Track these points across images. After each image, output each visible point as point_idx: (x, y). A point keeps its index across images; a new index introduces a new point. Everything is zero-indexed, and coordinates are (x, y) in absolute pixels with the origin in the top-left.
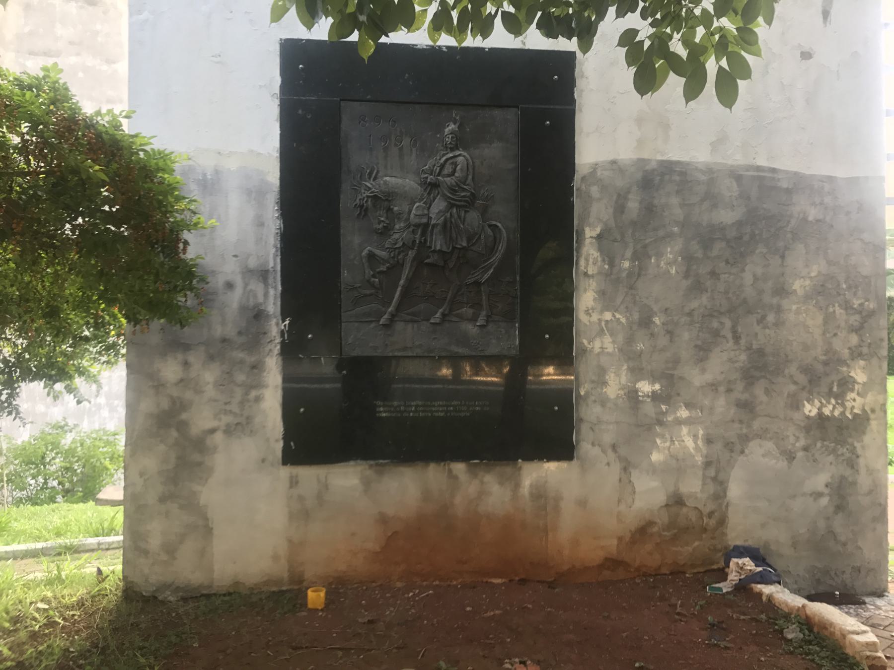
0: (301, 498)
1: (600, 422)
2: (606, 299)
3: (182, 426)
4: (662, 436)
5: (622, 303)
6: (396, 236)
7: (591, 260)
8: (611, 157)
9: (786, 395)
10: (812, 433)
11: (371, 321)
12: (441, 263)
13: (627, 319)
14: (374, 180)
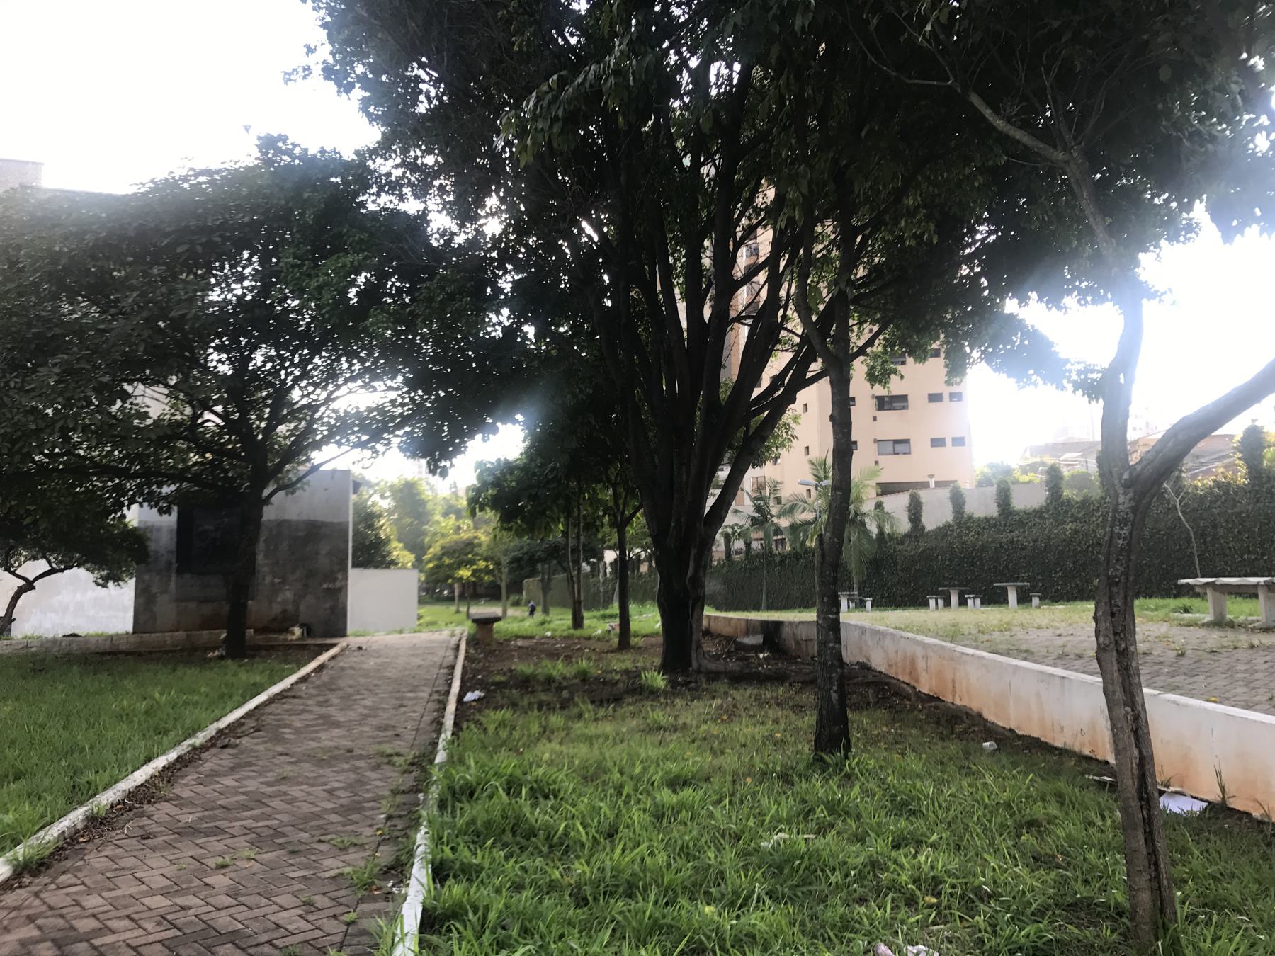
2: (266, 557)
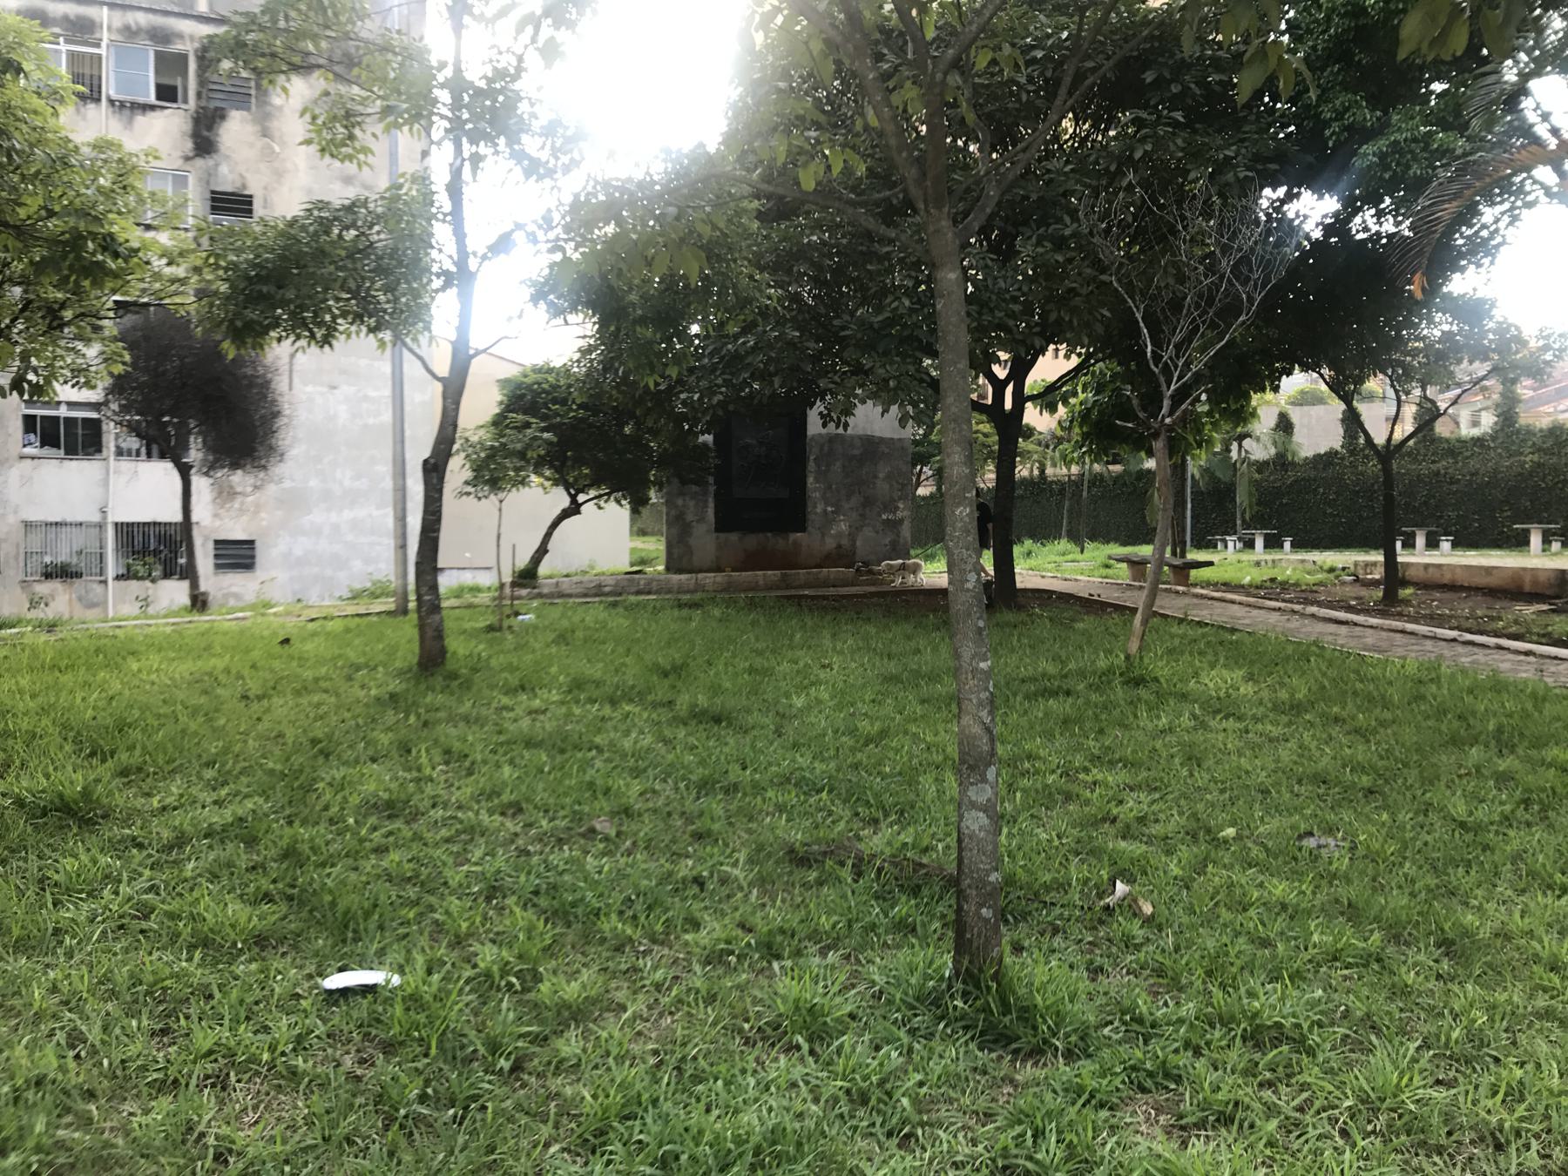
2: (817, 480)
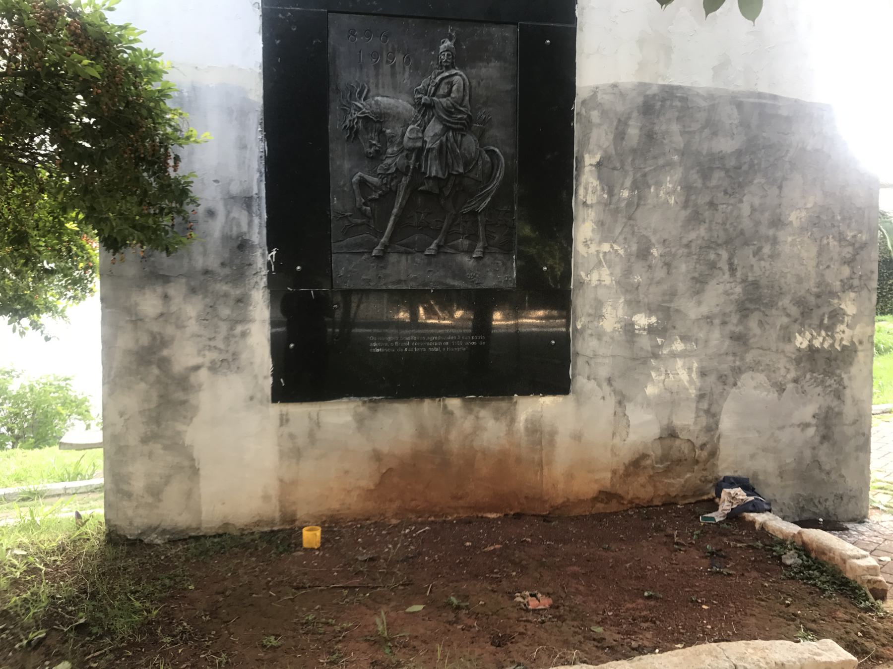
0: (292, 436)
1: (595, 356)
3: (164, 364)
4: (658, 369)
5: (620, 233)
6: (389, 161)
7: (590, 190)
8: (612, 81)
9: (778, 327)
10: (802, 365)
11: (363, 253)
12: (437, 191)
13: (626, 250)
14: (364, 100)
